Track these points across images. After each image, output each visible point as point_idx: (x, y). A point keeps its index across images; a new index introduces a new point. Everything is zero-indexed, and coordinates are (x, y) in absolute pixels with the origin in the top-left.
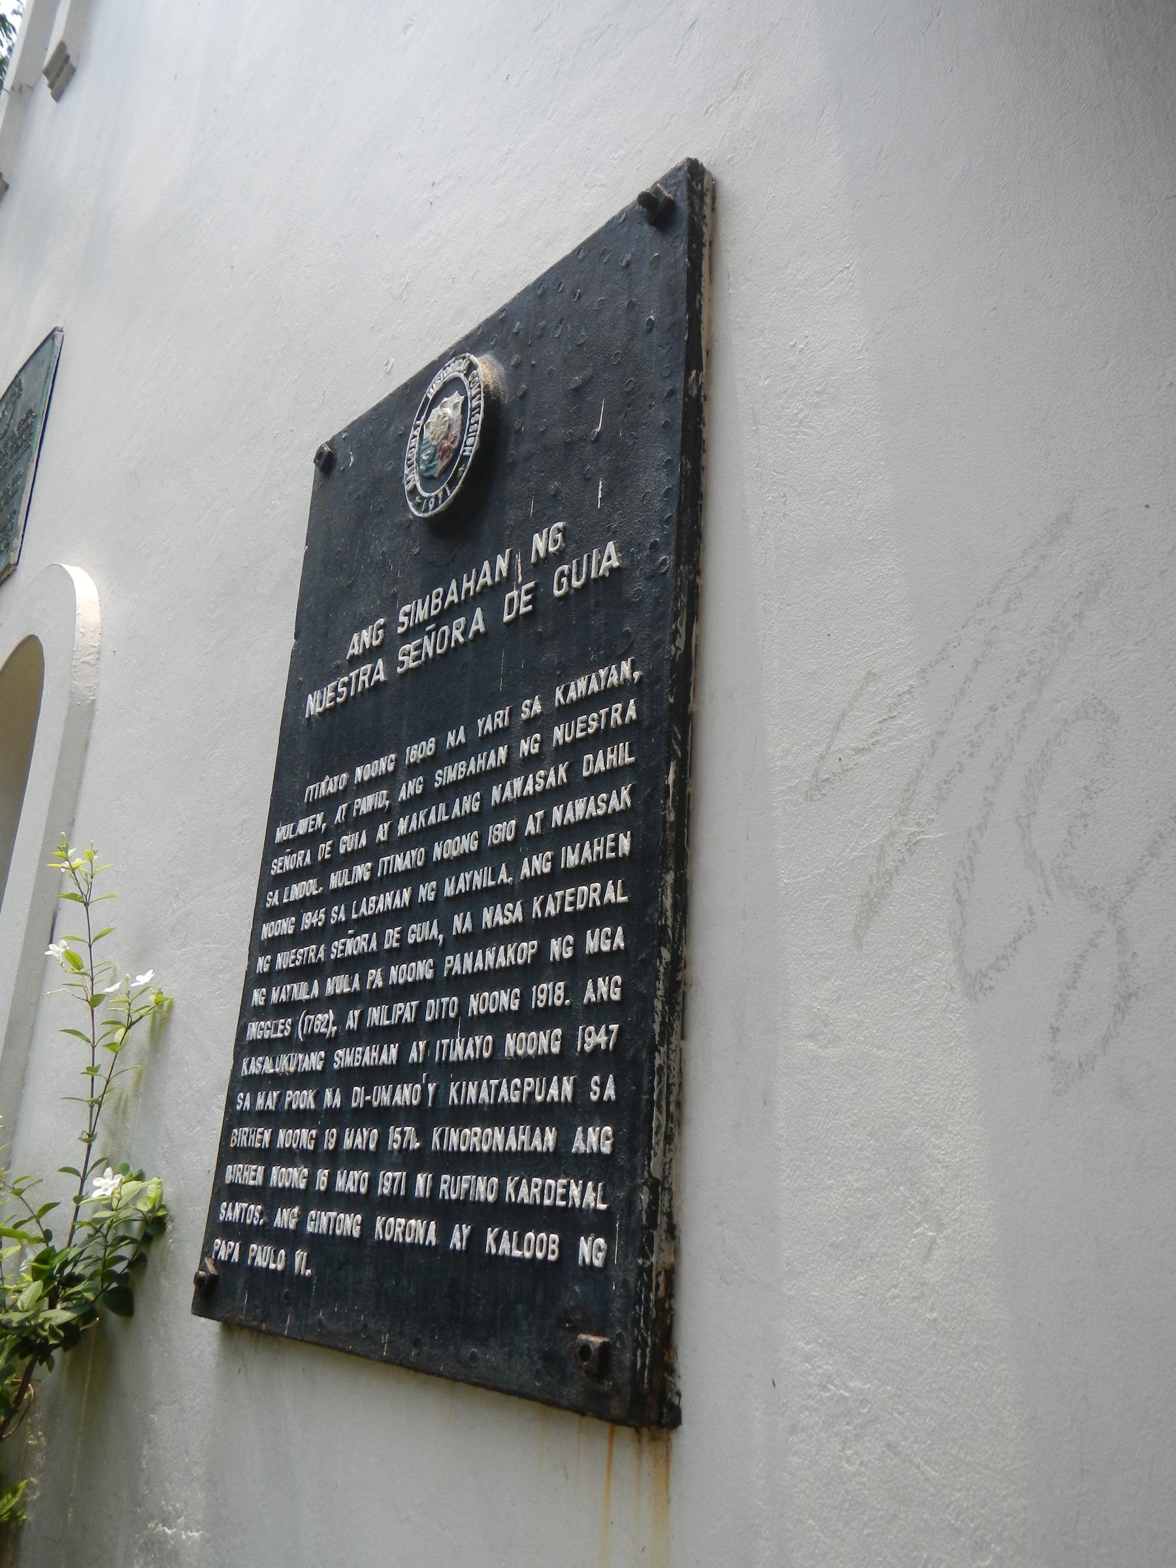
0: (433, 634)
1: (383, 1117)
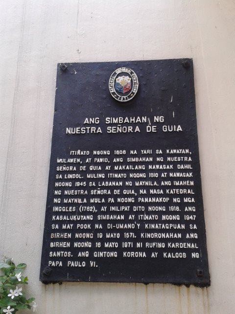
0: (121, 127)
1: (122, 231)
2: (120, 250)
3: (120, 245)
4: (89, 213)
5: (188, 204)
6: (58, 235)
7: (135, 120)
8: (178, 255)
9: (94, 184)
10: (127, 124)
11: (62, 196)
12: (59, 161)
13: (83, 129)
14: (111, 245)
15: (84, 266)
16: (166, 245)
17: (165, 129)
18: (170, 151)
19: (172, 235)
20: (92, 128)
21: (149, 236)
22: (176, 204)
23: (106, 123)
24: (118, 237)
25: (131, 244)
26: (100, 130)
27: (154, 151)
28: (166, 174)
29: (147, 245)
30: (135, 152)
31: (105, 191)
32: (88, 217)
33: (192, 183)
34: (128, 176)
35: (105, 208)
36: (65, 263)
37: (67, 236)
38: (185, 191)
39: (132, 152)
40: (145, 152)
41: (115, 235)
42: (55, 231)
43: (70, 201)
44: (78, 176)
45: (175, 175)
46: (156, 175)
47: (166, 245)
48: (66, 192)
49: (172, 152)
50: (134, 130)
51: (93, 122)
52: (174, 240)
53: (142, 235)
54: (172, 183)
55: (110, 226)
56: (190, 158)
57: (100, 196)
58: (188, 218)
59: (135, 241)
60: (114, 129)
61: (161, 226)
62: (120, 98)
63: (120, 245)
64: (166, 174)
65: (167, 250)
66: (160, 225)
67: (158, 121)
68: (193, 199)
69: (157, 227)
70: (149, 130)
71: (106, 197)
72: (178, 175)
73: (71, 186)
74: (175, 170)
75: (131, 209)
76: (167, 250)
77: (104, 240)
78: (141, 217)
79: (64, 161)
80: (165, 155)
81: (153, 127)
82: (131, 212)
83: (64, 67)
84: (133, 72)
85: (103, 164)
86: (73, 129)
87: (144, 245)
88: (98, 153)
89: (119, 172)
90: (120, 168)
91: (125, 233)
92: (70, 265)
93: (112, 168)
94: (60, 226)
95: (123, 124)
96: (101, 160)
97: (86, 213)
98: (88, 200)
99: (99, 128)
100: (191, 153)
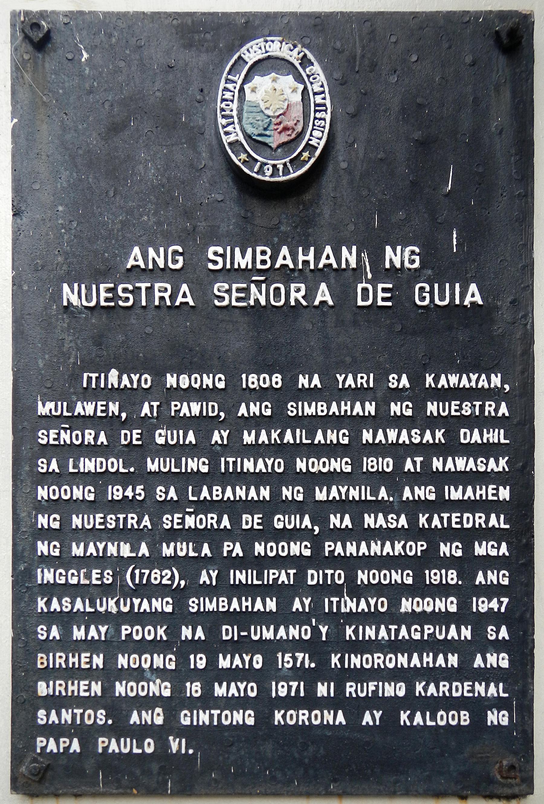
0: (264, 285)
1: (269, 648)
2: (264, 705)
3: (264, 690)
4: (162, 591)
5: (489, 563)
7: (317, 258)
9: (172, 494)
10: (287, 275)
12: (44, 409)
14: (233, 691)
15: (149, 750)
16: (411, 689)
17: (424, 295)
18: (436, 380)
19: (428, 659)
20: (157, 286)
21: (356, 661)
23: (211, 266)
24: (258, 666)
25: (299, 686)
27: (382, 378)
28: (419, 460)
29: (350, 688)
30: (316, 381)
31: (211, 519)
32: (157, 604)
33: (505, 494)
34: (290, 465)
35: (214, 574)
38: (480, 519)
39: (303, 381)
40: (350, 381)
41: (247, 658)
42: (48, 646)
43: (91, 550)
44: (115, 465)
45: (450, 465)
46: (387, 464)
47: (411, 689)
48: (77, 521)
49: (443, 382)
50: (310, 295)
52: (433, 675)
53: (335, 660)
54: (440, 493)
55: (229, 633)
56: (503, 404)
57: (195, 536)
58: (483, 605)
59: (310, 677)
60: (238, 290)
61: (397, 631)
63: (264, 690)
64: (419, 460)
65: (412, 702)
66: (393, 627)
67: (398, 266)
68: (504, 545)
69: (383, 633)
70: (365, 297)
71: (215, 536)
72: (461, 464)
73: (91, 497)
74: (451, 448)
75: (301, 576)
76: (412, 702)
77: (212, 675)
78: (331, 603)
79: (63, 409)
80: (419, 395)
81: (380, 286)
82: (300, 586)
83: (36, 26)
84: (310, 56)
87: (340, 689)
90: (263, 438)
91: (280, 655)
94: (66, 632)
95: (272, 274)
96: (196, 408)
97: (146, 590)
98: (154, 548)
99: (184, 287)
100: (507, 387)
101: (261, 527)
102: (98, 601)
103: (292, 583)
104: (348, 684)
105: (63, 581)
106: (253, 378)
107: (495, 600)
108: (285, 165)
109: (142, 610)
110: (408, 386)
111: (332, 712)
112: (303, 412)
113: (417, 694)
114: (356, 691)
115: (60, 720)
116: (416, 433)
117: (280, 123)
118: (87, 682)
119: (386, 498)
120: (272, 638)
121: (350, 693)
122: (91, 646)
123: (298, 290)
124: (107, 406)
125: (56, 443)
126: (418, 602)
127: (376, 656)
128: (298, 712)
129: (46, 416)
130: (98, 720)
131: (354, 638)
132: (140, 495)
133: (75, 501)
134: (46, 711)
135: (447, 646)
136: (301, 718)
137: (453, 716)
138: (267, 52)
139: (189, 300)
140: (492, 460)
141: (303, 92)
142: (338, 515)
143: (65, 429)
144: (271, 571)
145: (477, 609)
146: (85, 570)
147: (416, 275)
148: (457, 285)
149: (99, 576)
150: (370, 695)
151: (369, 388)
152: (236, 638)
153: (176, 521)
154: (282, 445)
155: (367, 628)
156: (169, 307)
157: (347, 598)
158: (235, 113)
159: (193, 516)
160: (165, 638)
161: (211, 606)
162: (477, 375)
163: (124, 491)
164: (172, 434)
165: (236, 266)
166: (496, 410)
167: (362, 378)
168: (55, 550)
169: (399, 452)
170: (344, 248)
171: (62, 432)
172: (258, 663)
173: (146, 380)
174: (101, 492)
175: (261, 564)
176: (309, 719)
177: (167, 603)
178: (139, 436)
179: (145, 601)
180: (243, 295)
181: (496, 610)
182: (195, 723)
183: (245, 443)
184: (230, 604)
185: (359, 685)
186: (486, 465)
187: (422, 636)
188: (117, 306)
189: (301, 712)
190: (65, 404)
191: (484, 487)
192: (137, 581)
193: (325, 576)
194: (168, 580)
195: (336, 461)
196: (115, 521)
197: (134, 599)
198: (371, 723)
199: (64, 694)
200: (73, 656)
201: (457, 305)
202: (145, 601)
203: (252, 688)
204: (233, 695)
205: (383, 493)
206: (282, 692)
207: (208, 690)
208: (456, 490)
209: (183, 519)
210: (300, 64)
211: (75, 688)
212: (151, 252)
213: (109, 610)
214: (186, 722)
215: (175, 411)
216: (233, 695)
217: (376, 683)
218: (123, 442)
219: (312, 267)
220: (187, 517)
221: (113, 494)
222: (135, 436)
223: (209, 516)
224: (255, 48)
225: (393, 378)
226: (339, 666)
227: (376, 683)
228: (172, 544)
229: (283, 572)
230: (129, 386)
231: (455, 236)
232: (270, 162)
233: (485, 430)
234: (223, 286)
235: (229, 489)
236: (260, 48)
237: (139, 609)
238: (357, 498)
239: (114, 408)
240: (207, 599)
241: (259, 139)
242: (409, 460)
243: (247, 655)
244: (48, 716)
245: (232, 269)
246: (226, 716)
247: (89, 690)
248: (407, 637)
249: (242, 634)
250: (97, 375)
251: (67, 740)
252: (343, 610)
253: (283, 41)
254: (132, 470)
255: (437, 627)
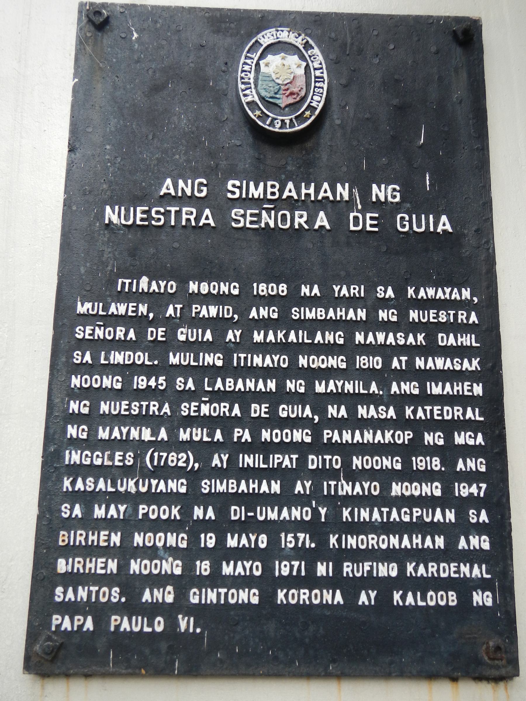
0: (273, 212)
1: (273, 529)
2: (268, 583)
3: (268, 569)
4: (177, 472)
5: (468, 451)
6: (80, 537)
7: (317, 192)
8: (434, 599)
9: (190, 385)
10: (292, 204)
11: (93, 419)
12: (83, 308)
13: (158, 212)
14: (240, 570)
15: (159, 629)
16: (402, 570)
17: (404, 223)
18: (417, 292)
19: (417, 540)
20: (184, 210)
21: (352, 542)
22: (433, 451)
23: (229, 195)
24: (263, 546)
25: (300, 566)
26: (208, 218)
27: (371, 289)
28: (404, 359)
29: (347, 568)
30: (316, 290)
31: (224, 408)
32: (172, 485)
33: (478, 390)
34: (294, 361)
35: (225, 458)
36: (101, 620)
37: (108, 540)
38: (458, 412)
39: (305, 290)
40: (344, 291)
41: (253, 538)
42: (70, 524)
43: (116, 434)
44: (142, 358)
45: (430, 364)
46: (377, 362)
47: (402, 570)
48: (104, 408)
50: (311, 220)
51: (189, 192)
52: (422, 556)
53: (333, 540)
54: (423, 388)
55: (237, 513)
56: (473, 314)
57: (210, 423)
58: (464, 490)
60: (252, 215)
61: (389, 514)
62: (274, 119)
63: (268, 569)
64: (404, 359)
65: (403, 582)
66: (385, 510)
67: (383, 200)
69: (376, 515)
70: (356, 224)
71: (226, 423)
72: (440, 363)
73: (119, 386)
74: (431, 349)
75: (302, 461)
76: (403, 582)
77: (221, 554)
78: (329, 486)
79: (99, 309)
80: (403, 304)
81: (368, 215)
82: (301, 471)
83: (98, 13)
84: (311, 42)
85: (219, 325)
86: (127, 211)
87: (338, 569)
88: (205, 288)
89: (264, 348)
90: (271, 337)
91: (283, 535)
92: (118, 627)
93: (247, 336)
94: (88, 510)
95: (279, 204)
96: (213, 311)
97: (164, 472)
98: (172, 433)
99: (207, 212)
100: (475, 299)
101: (267, 416)
102: (119, 481)
103: (294, 467)
104: (345, 564)
105: (88, 462)
106: (263, 286)
107: (475, 485)
108: (291, 120)
109: (158, 491)
110: (393, 296)
111: (331, 591)
112: (305, 316)
113: (408, 575)
114: (353, 571)
115: (76, 597)
116: (401, 336)
117: (287, 89)
118: (104, 560)
119: (377, 392)
120: (276, 519)
121: (347, 573)
122: (110, 524)
123: (301, 217)
124: (137, 307)
125: (91, 337)
126: (407, 487)
127: (370, 536)
128: (299, 591)
129: (84, 315)
130: (112, 598)
131: (350, 520)
132: (162, 385)
133: (104, 389)
134: (64, 588)
135: (434, 529)
136: (302, 597)
137: (442, 596)
138: (277, 38)
139: (211, 222)
140: (466, 361)
141: (306, 68)
142: (335, 406)
143: (100, 326)
144: (276, 456)
145: (459, 494)
146: (109, 452)
147: (397, 208)
148: (431, 216)
149: (121, 458)
150: (365, 575)
151: (360, 298)
152: (243, 519)
153: (193, 408)
154: (287, 343)
155: (362, 510)
156: (193, 227)
157: (344, 482)
158: (252, 81)
159: (208, 404)
160: (178, 518)
161: (221, 488)
162: (450, 289)
163: (148, 381)
164: (192, 332)
165: (250, 196)
166: (468, 318)
167: (354, 289)
168: (83, 433)
169: (386, 351)
170: (339, 185)
171: (97, 328)
172: (263, 542)
173: (172, 286)
174: (127, 382)
175: (267, 449)
176: (310, 598)
177: (182, 484)
178: (163, 334)
179: (162, 482)
180: (255, 219)
181: (476, 495)
182: (203, 602)
183: (255, 341)
184: (238, 486)
185: (355, 565)
186: (462, 364)
187: (411, 518)
188: (150, 225)
189: (302, 591)
190: (101, 304)
191: (460, 384)
192: (156, 463)
193: (324, 460)
194: (184, 462)
195: (333, 359)
196: (139, 408)
197: (152, 480)
198: (367, 603)
199: (82, 571)
200: (93, 534)
201: (432, 232)
202: (162, 482)
203: (257, 567)
204: (239, 573)
205: (373, 388)
206: (285, 571)
207: (216, 568)
208: (437, 386)
209: (199, 407)
210: (304, 48)
211: (93, 565)
212: (181, 183)
213: (129, 490)
214: (195, 600)
215: (196, 313)
216: (239, 573)
217: (370, 563)
218: (150, 338)
219: (313, 198)
220: (202, 405)
221: (138, 383)
222: (160, 333)
223: (222, 404)
224: (268, 35)
225: (381, 290)
226: (337, 547)
227: (370, 563)
228: (189, 430)
229: (287, 456)
230: (157, 291)
231: (428, 178)
232: (279, 117)
233: (459, 335)
234: (240, 212)
235: (240, 381)
236: (273, 35)
237: (156, 489)
238: (351, 391)
239: (143, 309)
240: (218, 481)
241: (271, 100)
242: (395, 359)
243: (253, 535)
244: (65, 593)
245: (247, 198)
246: (233, 595)
247: (105, 568)
248: (398, 519)
249: (249, 514)
250: (130, 281)
251: (81, 618)
252: (340, 493)
253: (290, 31)
254: (156, 362)
255: (425, 510)
